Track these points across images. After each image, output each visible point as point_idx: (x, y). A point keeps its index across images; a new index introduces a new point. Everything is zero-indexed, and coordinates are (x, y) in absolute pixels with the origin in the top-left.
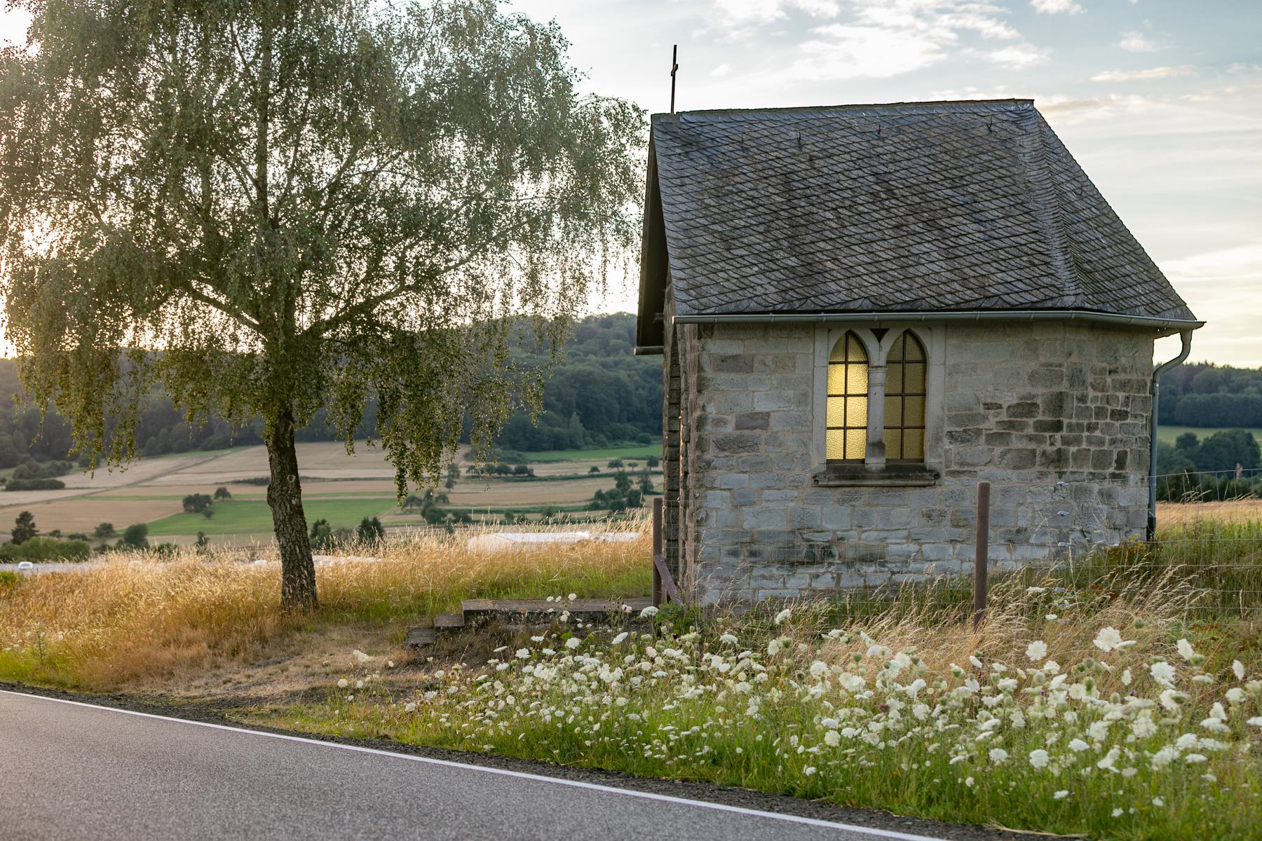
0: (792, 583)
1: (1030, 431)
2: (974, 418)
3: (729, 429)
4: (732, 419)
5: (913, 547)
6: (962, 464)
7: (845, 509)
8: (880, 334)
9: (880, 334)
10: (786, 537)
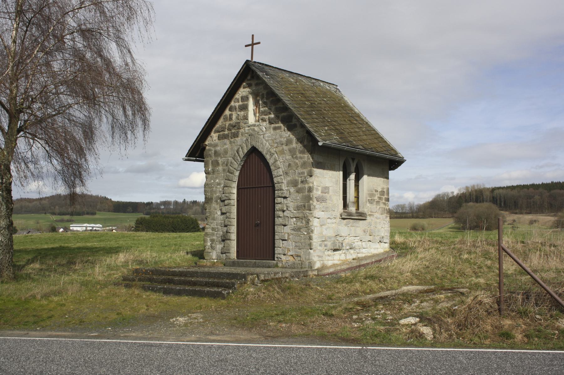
1: (384, 201)
3: (319, 193)
6: (371, 212)
7: (346, 228)
8: (353, 160)
9: (353, 160)
10: (333, 239)
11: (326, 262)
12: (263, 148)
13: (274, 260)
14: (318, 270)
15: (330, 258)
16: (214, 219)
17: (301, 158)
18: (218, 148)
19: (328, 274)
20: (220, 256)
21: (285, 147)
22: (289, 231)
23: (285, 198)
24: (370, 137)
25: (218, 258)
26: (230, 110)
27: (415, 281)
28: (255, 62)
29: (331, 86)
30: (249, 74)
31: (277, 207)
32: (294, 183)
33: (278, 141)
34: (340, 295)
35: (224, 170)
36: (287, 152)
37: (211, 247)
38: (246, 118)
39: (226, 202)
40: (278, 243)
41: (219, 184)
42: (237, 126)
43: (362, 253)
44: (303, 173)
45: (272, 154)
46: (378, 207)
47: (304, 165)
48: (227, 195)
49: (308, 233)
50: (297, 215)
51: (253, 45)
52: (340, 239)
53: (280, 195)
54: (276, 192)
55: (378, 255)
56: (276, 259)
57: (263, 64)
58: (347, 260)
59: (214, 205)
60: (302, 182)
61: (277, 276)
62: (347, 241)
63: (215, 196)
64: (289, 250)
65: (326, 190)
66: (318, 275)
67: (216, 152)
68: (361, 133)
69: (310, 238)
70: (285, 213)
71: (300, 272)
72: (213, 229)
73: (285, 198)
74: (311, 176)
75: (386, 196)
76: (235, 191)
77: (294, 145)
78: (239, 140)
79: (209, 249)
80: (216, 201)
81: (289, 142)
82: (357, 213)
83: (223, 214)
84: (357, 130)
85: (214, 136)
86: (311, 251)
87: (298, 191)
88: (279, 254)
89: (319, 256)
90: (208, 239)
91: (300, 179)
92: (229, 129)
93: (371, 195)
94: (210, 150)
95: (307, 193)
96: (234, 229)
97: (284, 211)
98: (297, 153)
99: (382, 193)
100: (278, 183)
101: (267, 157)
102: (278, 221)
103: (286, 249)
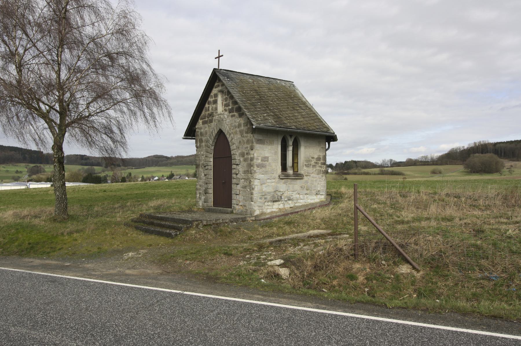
0: (274, 207)
1: (320, 165)
2: (310, 161)
3: (259, 161)
4: (260, 158)
5: (298, 196)
6: (308, 173)
7: (285, 185)
8: (291, 136)
9: (291, 136)
10: (272, 194)
11: (265, 210)
12: (225, 130)
14: (256, 216)
15: (269, 207)
17: (246, 137)
18: (202, 130)
19: (264, 219)
21: (238, 130)
23: (237, 165)
24: (307, 119)
25: (203, 205)
26: (208, 104)
27: (323, 226)
28: (221, 69)
29: (287, 83)
30: (216, 78)
31: (233, 171)
32: (242, 155)
34: (258, 237)
35: (205, 145)
36: (238, 132)
37: (200, 198)
38: (216, 109)
39: (206, 167)
40: (234, 196)
41: (203, 155)
42: (211, 115)
43: (300, 203)
44: (247, 147)
46: (315, 169)
47: (248, 142)
49: (250, 190)
50: (244, 177)
51: (219, 57)
52: (279, 194)
53: (235, 163)
55: (313, 204)
57: (228, 70)
58: (285, 208)
60: (247, 154)
61: (218, 222)
62: (285, 195)
64: (240, 202)
65: (265, 159)
66: (255, 220)
67: (201, 133)
68: (300, 117)
69: (252, 194)
70: (238, 176)
71: (239, 218)
72: (200, 186)
73: (237, 165)
74: (252, 150)
75: (322, 161)
76: (212, 160)
77: (242, 128)
78: (213, 124)
81: (239, 125)
82: (293, 174)
83: (205, 175)
84: (296, 114)
85: (200, 121)
86: (253, 203)
87: (245, 160)
89: (259, 206)
92: (208, 118)
93: (308, 161)
94: (198, 132)
95: (249, 162)
96: (211, 186)
97: (237, 174)
99: (319, 159)
100: (234, 154)
101: (228, 136)
102: (234, 181)
103: (238, 200)
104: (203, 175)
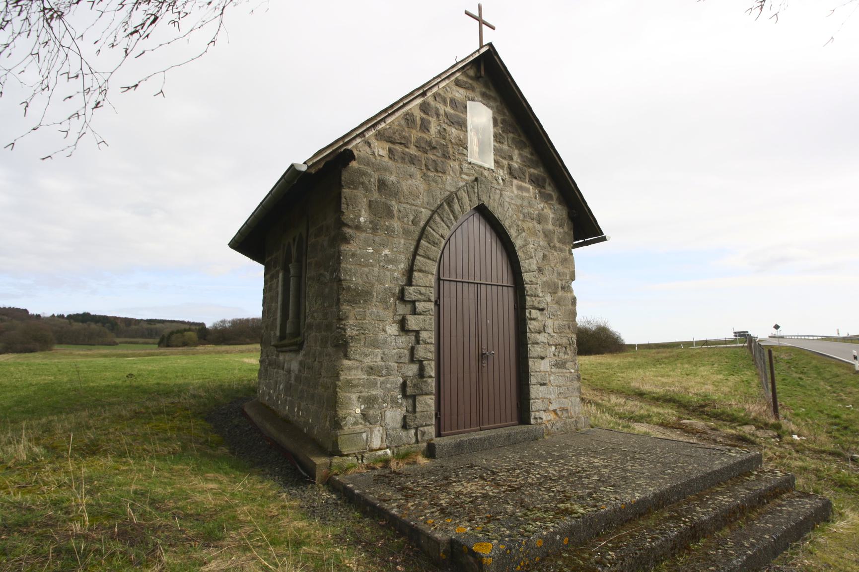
13: (529, 423)
16: (375, 344)
20: (401, 437)
22: (548, 369)
31: (532, 325)
33: (525, 211)
36: (541, 234)
45: (520, 230)
48: (423, 290)
54: (528, 298)
56: (532, 421)
59: (375, 308)
63: (378, 287)
72: (371, 370)
73: (542, 310)
77: (550, 227)
79: (356, 423)
80: (384, 301)
81: (540, 219)
88: (538, 411)
90: (354, 397)
91: (560, 282)
98: (556, 241)
100: (532, 283)
101: (512, 233)
104: (393, 329)
